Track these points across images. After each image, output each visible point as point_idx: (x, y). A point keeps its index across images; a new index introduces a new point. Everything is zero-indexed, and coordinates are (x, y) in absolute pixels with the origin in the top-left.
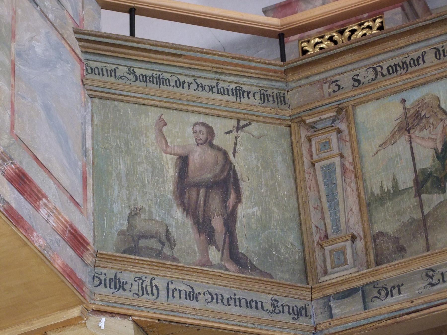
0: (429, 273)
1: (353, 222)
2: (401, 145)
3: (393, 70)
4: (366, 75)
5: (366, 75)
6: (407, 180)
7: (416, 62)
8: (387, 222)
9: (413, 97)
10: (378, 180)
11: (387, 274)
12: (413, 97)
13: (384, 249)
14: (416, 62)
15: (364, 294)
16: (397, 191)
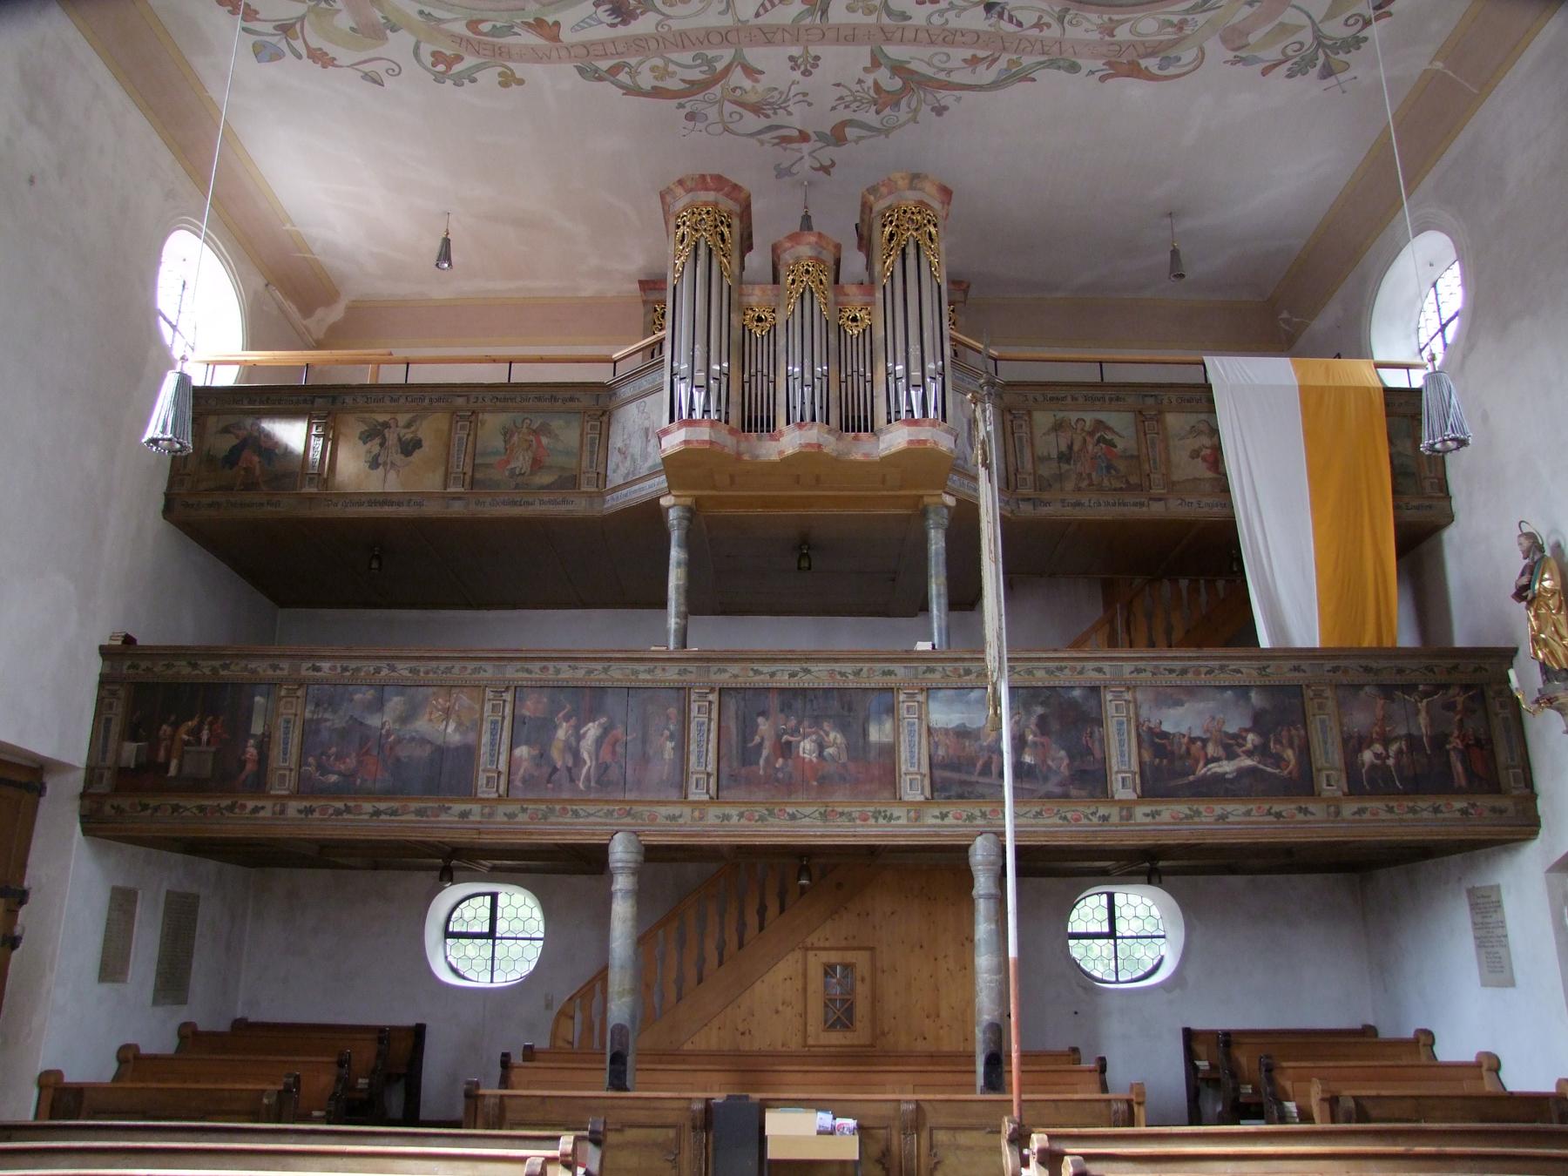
0: (1063, 501)
1: (1029, 466)
2: (1053, 435)
3: (1052, 399)
4: (1040, 398)
5: (1040, 398)
6: (1054, 455)
7: (1064, 398)
8: (1046, 471)
9: (1060, 415)
10: (1041, 450)
11: (1046, 496)
12: (1060, 415)
13: (1042, 484)
14: (1064, 398)
15: (1035, 502)
16: (1049, 458)
